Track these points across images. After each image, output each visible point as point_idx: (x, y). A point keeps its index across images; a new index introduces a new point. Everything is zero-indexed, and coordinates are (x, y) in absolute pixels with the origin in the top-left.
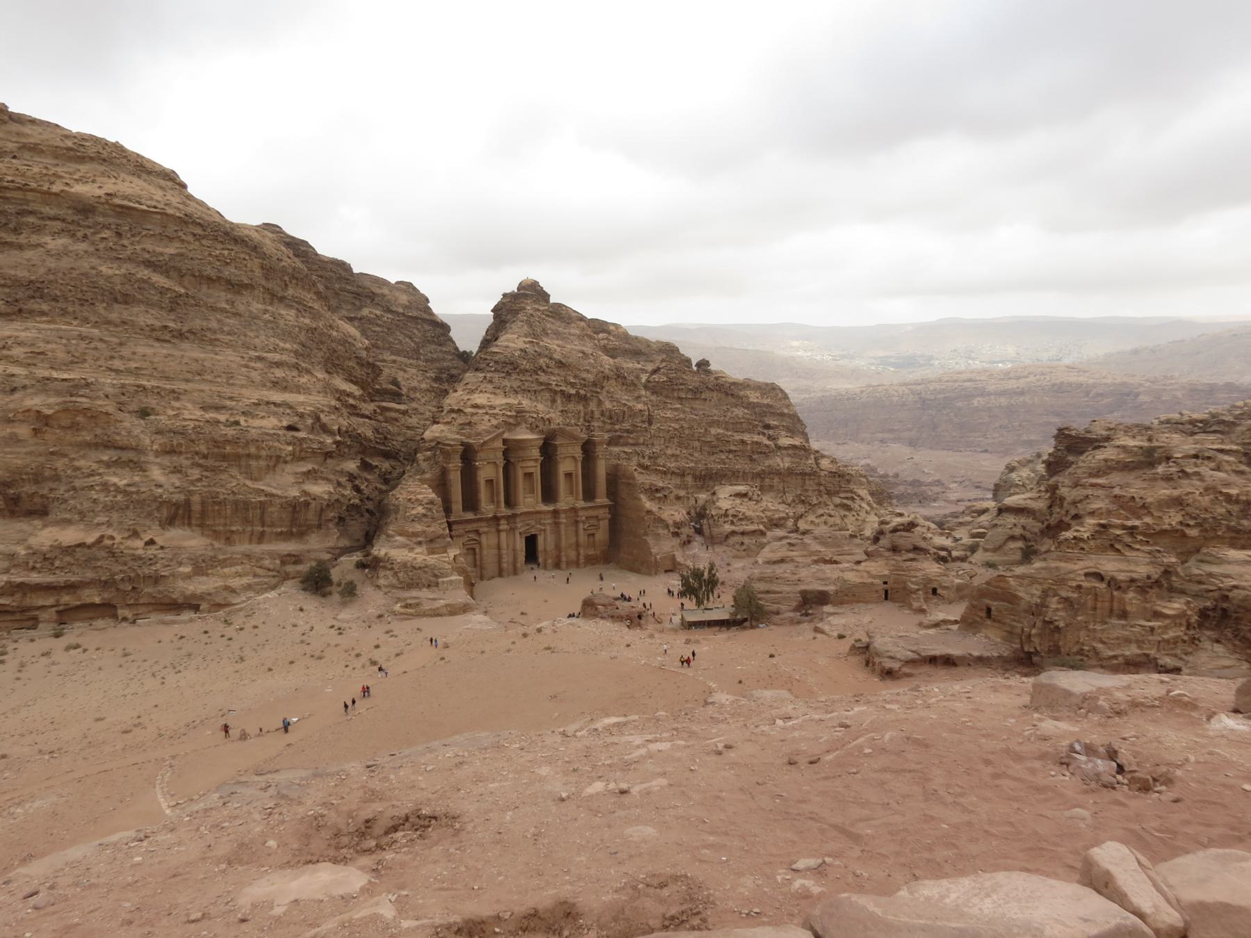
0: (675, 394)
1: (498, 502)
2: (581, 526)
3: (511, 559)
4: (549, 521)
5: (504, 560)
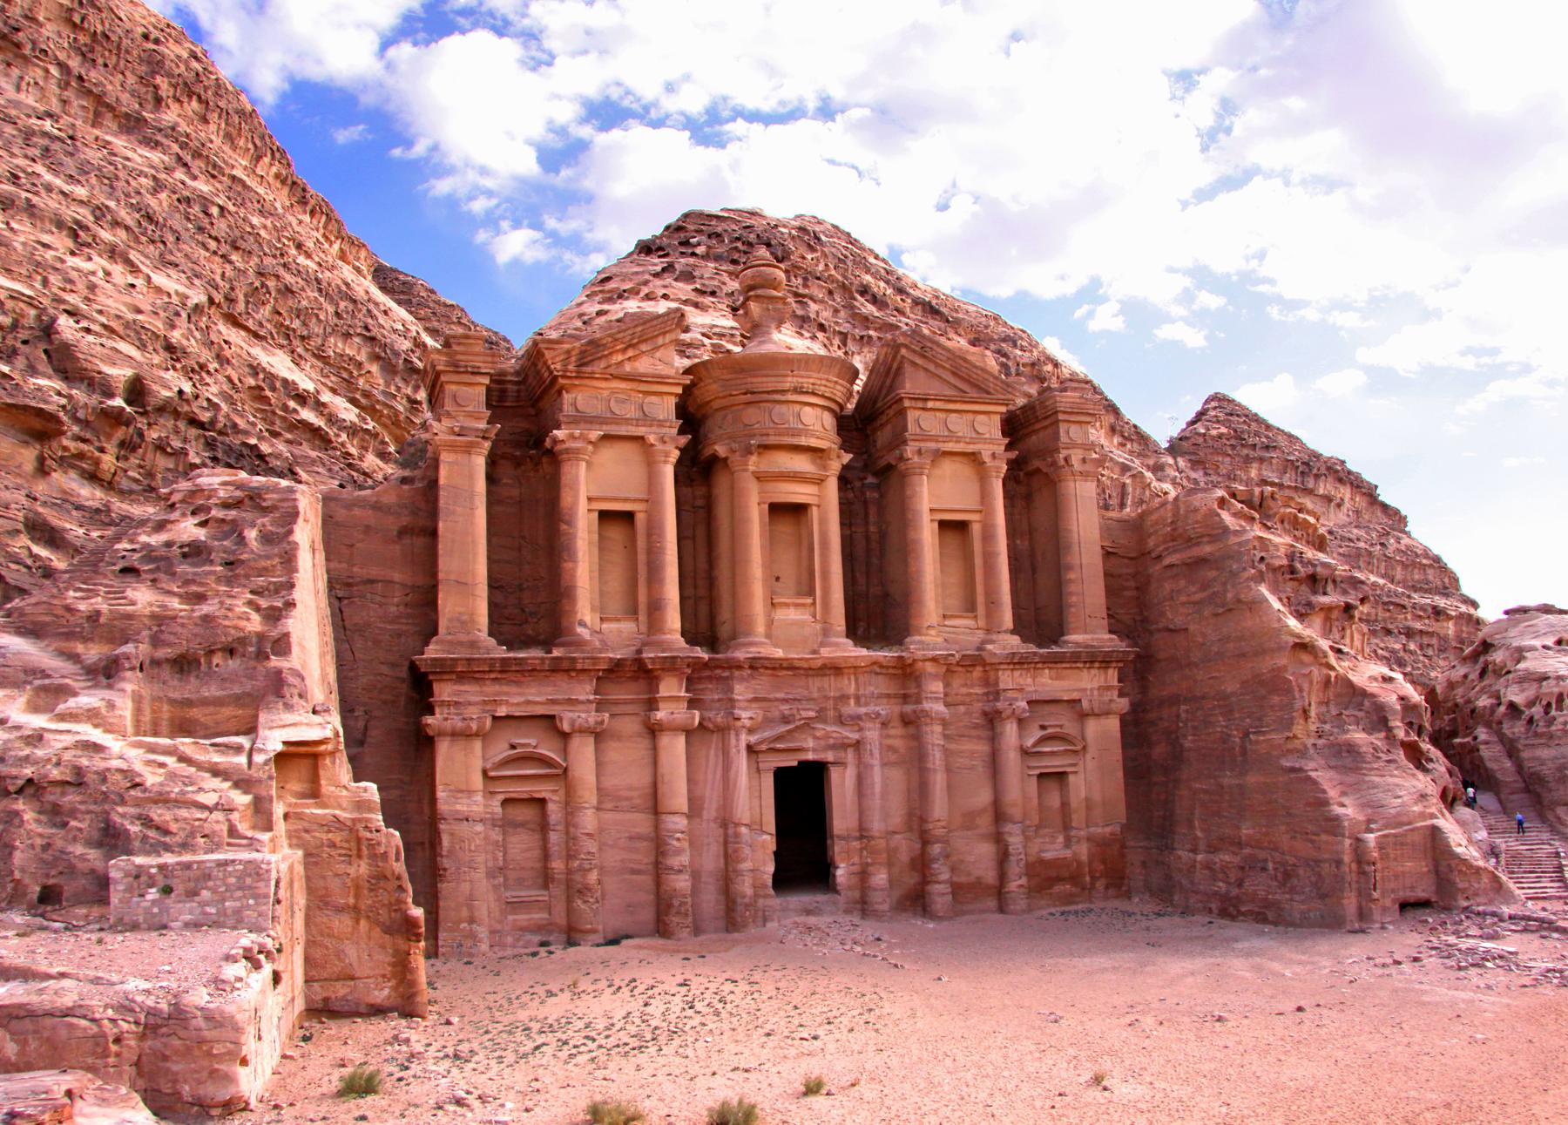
0: (1253, 473)
1: (656, 608)
2: (1010, 730)
3: (711, 861)
4: (883, 709)
5: (675, 861)
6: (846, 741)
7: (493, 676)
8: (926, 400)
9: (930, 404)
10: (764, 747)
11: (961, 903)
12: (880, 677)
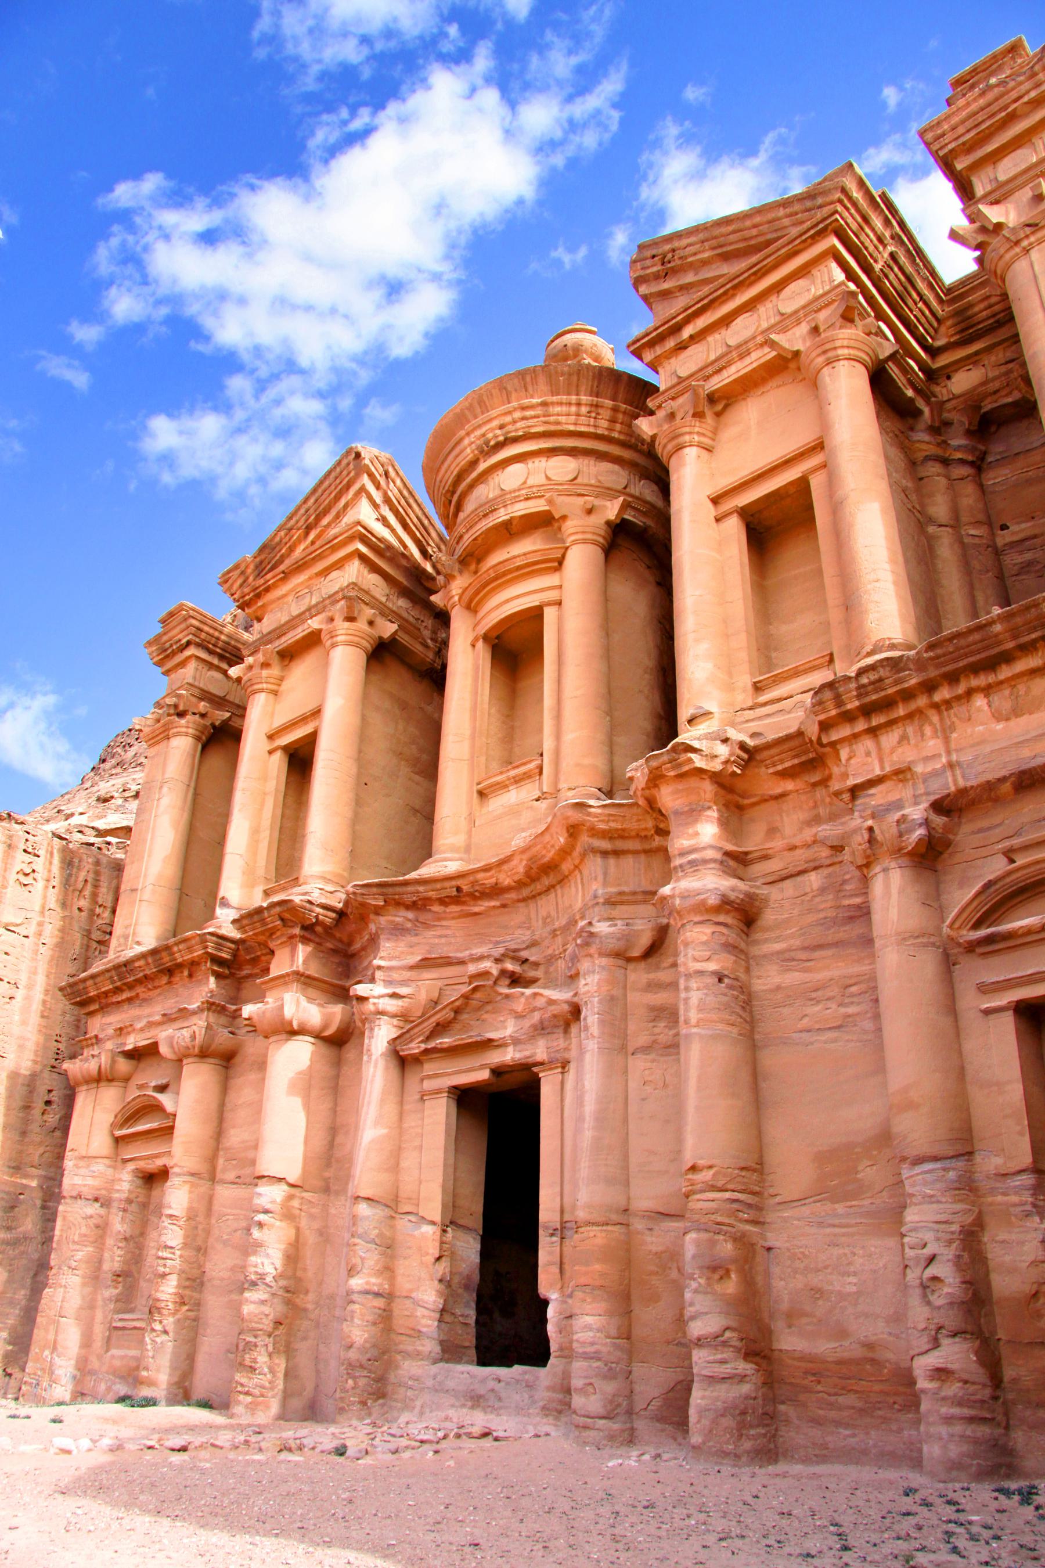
6: (555, 1009)
7: (125, 995)
8: (677, 329)
9: (687, 332)
10: (415, 1047)
11: (817, 1422)
12: (628, 861)
